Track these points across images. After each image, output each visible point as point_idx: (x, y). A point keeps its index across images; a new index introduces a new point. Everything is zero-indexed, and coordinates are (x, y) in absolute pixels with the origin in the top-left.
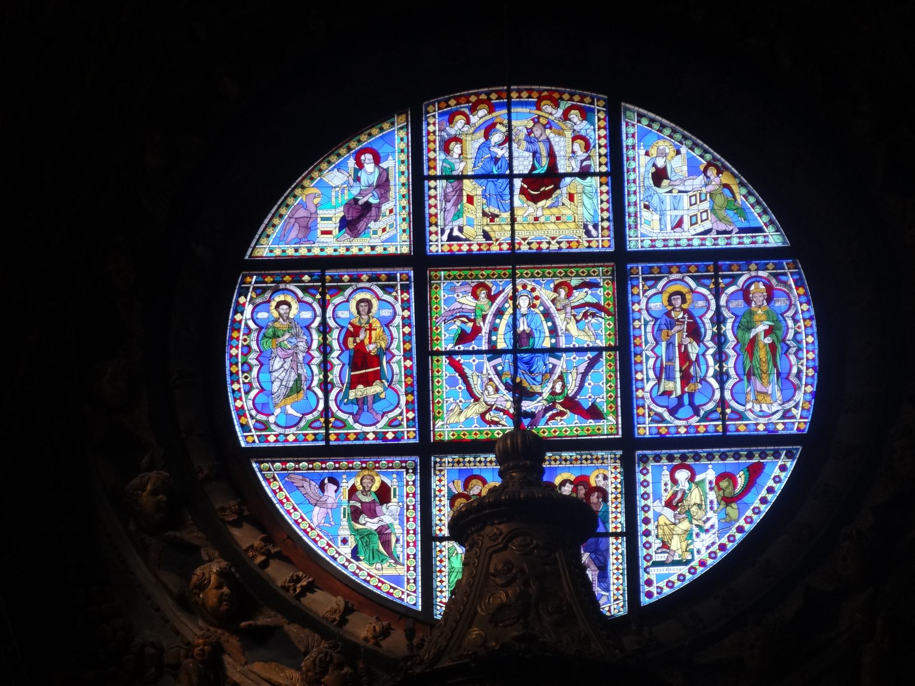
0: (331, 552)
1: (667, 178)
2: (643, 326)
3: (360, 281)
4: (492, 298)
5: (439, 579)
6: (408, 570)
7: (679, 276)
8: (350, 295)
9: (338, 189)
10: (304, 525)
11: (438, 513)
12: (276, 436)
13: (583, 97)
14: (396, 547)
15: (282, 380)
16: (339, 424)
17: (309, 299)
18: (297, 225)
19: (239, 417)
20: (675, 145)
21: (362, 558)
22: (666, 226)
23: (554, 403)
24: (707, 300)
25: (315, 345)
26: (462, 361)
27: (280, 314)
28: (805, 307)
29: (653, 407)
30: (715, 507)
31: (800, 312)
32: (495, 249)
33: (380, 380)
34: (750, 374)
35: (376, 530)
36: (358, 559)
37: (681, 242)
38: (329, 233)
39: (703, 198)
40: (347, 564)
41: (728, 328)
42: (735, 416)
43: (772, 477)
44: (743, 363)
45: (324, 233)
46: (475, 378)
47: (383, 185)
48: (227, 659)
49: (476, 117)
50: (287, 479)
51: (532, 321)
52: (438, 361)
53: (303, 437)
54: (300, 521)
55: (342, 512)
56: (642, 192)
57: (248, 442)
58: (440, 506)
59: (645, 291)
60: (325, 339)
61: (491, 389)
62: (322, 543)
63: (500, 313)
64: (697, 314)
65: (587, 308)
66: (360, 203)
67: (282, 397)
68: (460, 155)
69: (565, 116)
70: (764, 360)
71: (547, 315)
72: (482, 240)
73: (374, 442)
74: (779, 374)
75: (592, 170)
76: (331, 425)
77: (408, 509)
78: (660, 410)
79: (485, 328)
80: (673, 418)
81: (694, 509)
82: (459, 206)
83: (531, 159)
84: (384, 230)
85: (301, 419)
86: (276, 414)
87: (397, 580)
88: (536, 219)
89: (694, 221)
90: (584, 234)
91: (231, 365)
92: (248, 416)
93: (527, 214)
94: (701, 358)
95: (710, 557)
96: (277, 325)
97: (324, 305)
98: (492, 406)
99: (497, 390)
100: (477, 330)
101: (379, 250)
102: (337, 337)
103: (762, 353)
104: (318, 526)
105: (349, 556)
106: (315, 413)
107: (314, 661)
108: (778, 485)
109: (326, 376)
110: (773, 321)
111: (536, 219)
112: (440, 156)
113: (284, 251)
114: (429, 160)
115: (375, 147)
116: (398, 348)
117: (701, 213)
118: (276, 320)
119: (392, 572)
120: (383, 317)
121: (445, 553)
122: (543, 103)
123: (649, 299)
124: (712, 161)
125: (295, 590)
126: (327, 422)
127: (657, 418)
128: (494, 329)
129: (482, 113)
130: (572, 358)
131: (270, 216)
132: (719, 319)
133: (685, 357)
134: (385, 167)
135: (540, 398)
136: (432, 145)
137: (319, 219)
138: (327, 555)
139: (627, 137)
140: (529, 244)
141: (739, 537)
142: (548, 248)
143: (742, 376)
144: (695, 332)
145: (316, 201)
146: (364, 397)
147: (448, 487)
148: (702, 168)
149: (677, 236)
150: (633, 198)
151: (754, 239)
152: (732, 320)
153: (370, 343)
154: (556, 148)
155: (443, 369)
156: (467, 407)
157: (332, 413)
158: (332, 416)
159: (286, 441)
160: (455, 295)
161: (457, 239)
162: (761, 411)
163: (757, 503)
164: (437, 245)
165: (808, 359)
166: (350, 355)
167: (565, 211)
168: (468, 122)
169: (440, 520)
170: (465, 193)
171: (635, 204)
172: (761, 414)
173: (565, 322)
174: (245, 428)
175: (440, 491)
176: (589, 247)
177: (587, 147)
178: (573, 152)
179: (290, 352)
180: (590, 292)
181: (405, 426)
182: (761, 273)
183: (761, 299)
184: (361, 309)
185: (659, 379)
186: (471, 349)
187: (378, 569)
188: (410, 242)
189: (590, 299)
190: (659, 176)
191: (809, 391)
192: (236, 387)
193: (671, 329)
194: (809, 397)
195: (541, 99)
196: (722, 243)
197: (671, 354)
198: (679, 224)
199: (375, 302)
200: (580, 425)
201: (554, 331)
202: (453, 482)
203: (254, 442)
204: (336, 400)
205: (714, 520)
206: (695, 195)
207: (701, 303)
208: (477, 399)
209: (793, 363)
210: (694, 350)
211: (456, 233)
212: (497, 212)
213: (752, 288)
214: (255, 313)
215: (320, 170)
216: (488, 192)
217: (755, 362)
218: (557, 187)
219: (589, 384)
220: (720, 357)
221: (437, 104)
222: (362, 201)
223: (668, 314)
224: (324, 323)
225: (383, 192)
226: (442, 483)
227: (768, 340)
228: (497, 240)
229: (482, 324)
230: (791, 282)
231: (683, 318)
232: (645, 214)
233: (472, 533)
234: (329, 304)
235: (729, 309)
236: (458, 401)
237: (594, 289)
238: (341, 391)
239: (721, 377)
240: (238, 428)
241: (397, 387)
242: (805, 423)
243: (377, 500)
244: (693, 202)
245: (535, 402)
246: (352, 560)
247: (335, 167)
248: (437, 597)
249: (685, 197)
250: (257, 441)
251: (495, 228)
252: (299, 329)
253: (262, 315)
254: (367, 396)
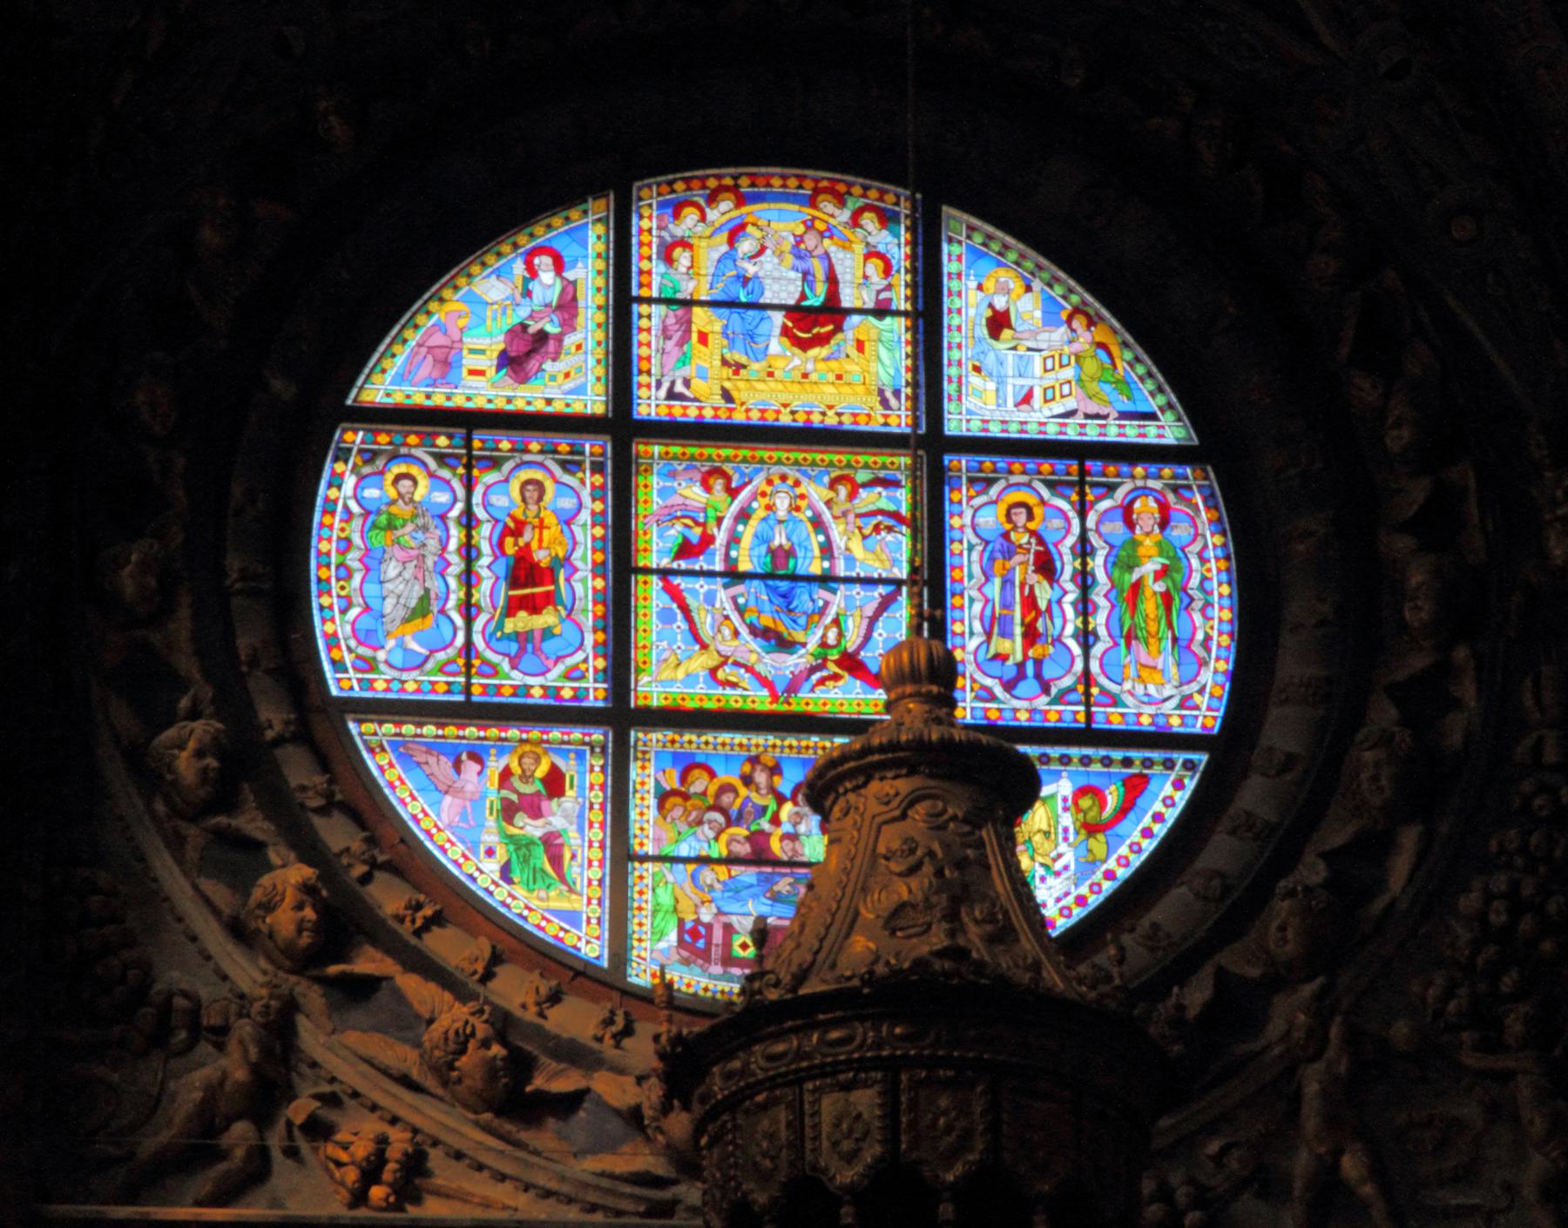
0: (469, 868)
1: (1009, 326)
2: (965, 553)
3: (526, 451)
4: (733, 493)
5: (636, 921)
6: (589, 902)
7: (1024, 479)
8: (511, 471)
9: (496, 307)
10: (426, 824)
11: (638, 818)
12: (388, 681)
13: (882, 192)
14: (570, 866)
15: (399, 597)
16: (487, 669)
17: (445, 473)
18: (430, 358)
19: (329, 648)
20: (1024, 278)
21: (516, 880)
22: (1005, 401)
23: (825, 660)
24: (1067, 519)
25: (453, 545)
26: (683, 586)
27: (400, 494)
28: (1218, 540)
29: (978, 676)
30: (1071, 838)
31: (1211, 546)
32: (739, 417)
33: (555, 605)
34: (1130, 638)
35: (540, 838)
36: (510, 881)
37: (1028, 427)
38: (481, 373)
39: (1065, 361)
40: (492, 888)
41: (1097, 564)
42: (1105, 700)
43: (1161, 798)
44: (1120, 619)
45: (472, 372)
46: (703, 613)
47: (567, 306)
48: (302, 1023)
49: (715, 212)
50: (401, 750)
51: (793, 531)
52: (645, 583)
53: (430, 687)
54: (421, 816)
55: (488, 805)
56: (970, 346)
57: (342, 689)
58: (642, 806)
59: (970, 498)
60: (469, 537)
61: (727, 632)
62: (456, 852)
63: (744, 515)
64: (1050, 538)
65: (880, 518)
66: (531, 330)
67: (398, 622)
68: (689, 268)
69: (855, 221)
70: (1152, 616)
71: (818, 523)
72: (719, 401)
73: (542, 702)
74: (1175, 640)
75: (894, 307)
76: (474, 670)
77: (591, 807)
78: (988, 682)
79: (721, 537)
80: (1008, 696)
81: (1038, 838)
82: (685, 348)
83: (800, 283)
84: (567, 375)
85: (427, 659)
86: (388, 648)
87: (572, 918)
88: (805, 376)
89: (1049, 394)
90: (878, 404)
91: (319, 566)
92: (344, 648)
93: (791, 366)
94: (1055, 608)
95: (1061, 914)
96: (393, 509)
97: (469, 485)
98: (727, 658)
99: (736, 634)
100: (707, 540)
101: (558, 407)
102: (488, 534)
103: (1149, 606)
104: (449, 826)
105: (496, 877)
106: (451, 652)
107: (446, 1032)
108: (1170, 810)
109: (469, 595)
110: (1168, 558)
111: (805, 376)
112: (658, 267)
113: (408, 397)
114: (641, 272)
115: (556, 245)
116: (584, 558)
117: (1061, 385)
118: (393, 502)
119: (564, 905)
120: (563, 509)
121: (648, 880)
122: (820, 198)
123: (976, 510)
124: (1081, 307)
125: (413, 921)
126: (468, 666)
127: (983, 694)
128: (734, 539)
129: (726, 205)
130: (854, 593)
131: (387, 340)
132: (1084, 549)
133: (1030, 602)
134: (571, 279)
135: (803, 651)
136: (645, 251)
137: (465, 352)
138: (462, 872)
139: (950, 260)
140: (793, 413)
141: (1108, 887)
142: (822, 422)
143: (1117, 640)
144: (1046, 566)
145: (462, 323)
146: (526, 633)
147: (656, 780)
148: (1064, 316)
149: (1022, 416)
150: (955, 355)
151: (1142, 431)
152: (1105, 552)
153: (540, 547)
154: (838, 269)
155: (650, 597)
156: (689, 658)
157: (477, 651)
158: (477, 657)
159: (403, 690)
160: (675, 484)
161: (681, 397)
162: (1147, 695)
163: (1136, 836)
164: (649, 404)
165: (1221, 620)
166: (507, 566)
167: (848, 366)
168: (703, 218)
169: (642, 829)
170: (694, 328)
171: (960, 363)
172: (1146, 699)
173: (845, 538)
174: (338, 665)
175: (643, 784)
176: (886, 424)
177: (888, 271)
178: (866, 277)
179: (414, 553)
180: (884, 493)
181: (591, 679)
182: (1151, 483)
183: (1151, 522)
184: (527, 494)
185: (989, 634)
186: (697, 567)
187: (541, 899)
188: (607, 395)
189: (884, 504)
190: (998, 323)
191: (1221, 669)
192: (325, 601)
193: (1010, 559)
194: (1221, 679)
195: (817, 192)
196: (1092, 434)
197: (1009, 598)
198: (1027, 399)
199: (549, 485)
200: (862, 696)
201: (827, 550)
202: (664, 771)
203: (351, 688)
204: (483, 633)
205: (1069, 858)
206: (1053, 357)
207: (1058, 523)
208: (704, 646)
209: (1197, 624)
210: (1044, 594)
211: (679, 388)
212: (743, 360)
213: (1137, 505)
214: (359, 490)
215: (469, 276)
216: (730, 327)
217: (1139, 619)
218: (839, 328)
219: (880, 635)
220: (1085, 607)
221: (654, 188)
222: (534, 327)
223: (1006, 535)
224: (468, 512)
225: (567, 316)
226: (647, 772)
227: (1160, 587)
228: (743, 404)
229: (715, 530)
230: (1198, 499)
231: (1029, 543)
232: (975, 379)
233: (846, 791)
234: (476, 483)
235: (1100, 535)
236: (675, 647)
237: (892, 489)
238: (492, 618)
239: (1086, 638)
240: (326, 666)
241: (580, 618)
242: (1215, 718)
243: (543, 791)
244: (1049, 365)
245: (795, 656)
246: (501, 882)
247: (492, 273)
248: (633, 948)
249: (1037, 359)
250: (356, 687)
251: (741, 385)
252: (428, 519)
253: (371, 493)
254: (532, 631)
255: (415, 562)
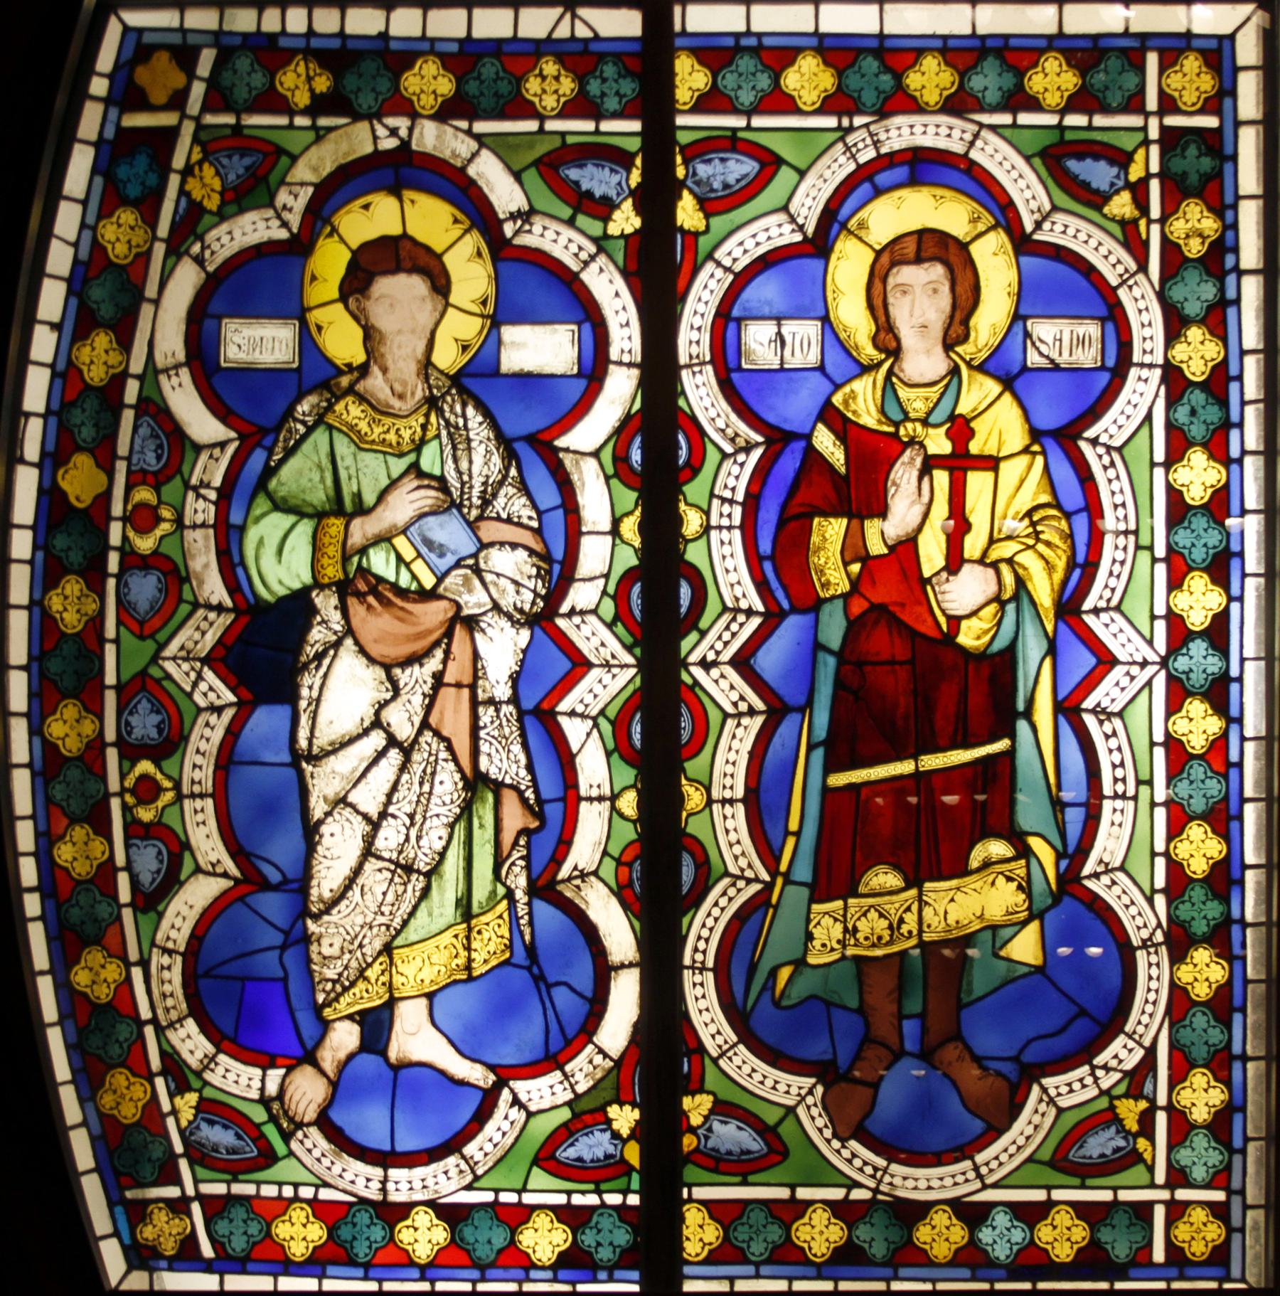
153: (954, 562)
255: (434, 664)
